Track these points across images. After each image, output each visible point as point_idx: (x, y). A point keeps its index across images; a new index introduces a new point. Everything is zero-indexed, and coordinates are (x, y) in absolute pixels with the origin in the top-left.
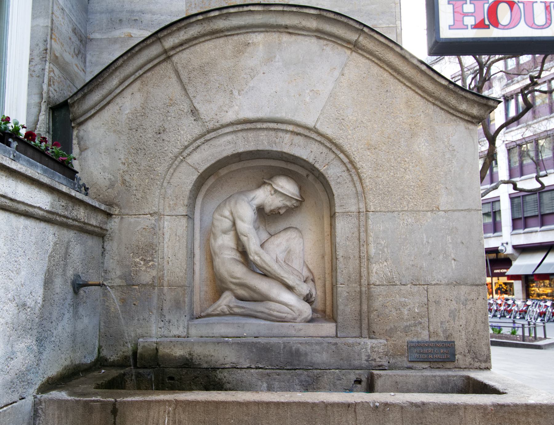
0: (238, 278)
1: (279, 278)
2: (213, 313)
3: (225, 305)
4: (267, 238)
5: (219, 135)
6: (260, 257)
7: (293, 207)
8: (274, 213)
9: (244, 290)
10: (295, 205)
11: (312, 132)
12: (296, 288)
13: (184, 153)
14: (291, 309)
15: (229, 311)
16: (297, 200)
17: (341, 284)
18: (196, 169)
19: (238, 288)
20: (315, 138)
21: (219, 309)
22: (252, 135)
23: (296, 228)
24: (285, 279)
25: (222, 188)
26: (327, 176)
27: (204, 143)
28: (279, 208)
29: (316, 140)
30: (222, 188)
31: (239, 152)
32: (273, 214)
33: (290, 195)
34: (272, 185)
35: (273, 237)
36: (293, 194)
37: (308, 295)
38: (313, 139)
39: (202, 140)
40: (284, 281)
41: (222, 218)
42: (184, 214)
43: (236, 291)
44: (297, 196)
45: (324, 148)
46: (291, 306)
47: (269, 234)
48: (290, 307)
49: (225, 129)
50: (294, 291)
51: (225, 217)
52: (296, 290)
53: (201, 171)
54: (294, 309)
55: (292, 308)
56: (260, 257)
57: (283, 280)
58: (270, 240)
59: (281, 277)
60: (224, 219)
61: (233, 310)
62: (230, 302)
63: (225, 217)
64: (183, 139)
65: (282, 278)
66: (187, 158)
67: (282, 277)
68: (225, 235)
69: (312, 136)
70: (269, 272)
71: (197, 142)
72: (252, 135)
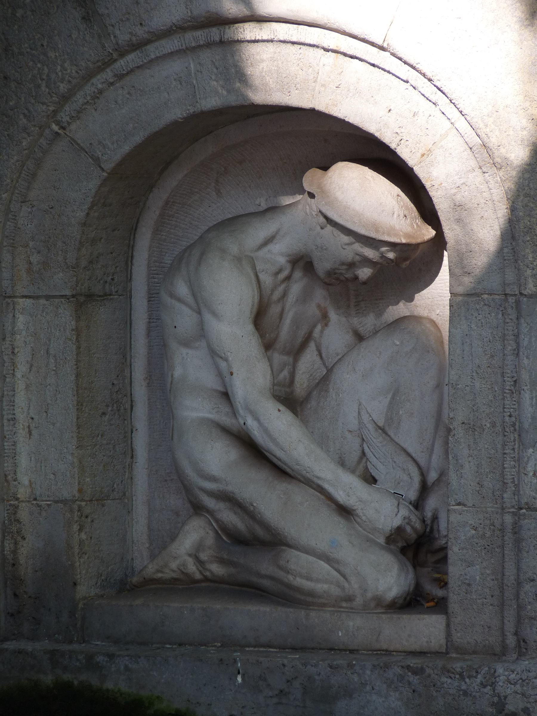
0: (213, 479)
1: (313, 482)
2: (160, 575)
12: (359, 512)
13: (62, 114)
17: (459, 504)
21: (174, 565)
25: (218, 192)
27: (112, 84)
30: (218, 192)
39: (108, 74)
41: (173, 301)
42: (68, 293)
46: (338, 562)
48: (336, 566)
50: (356, 518)
51: (179, 300)
55: (342, 568)
60: (178, 305)
61: (207, 570)
62: (200, 546)
63: (179, 300)
64: (53, 76)
66: (73, 127)
67: (318, 478)
68: (190, 352)
71: (94, 80)
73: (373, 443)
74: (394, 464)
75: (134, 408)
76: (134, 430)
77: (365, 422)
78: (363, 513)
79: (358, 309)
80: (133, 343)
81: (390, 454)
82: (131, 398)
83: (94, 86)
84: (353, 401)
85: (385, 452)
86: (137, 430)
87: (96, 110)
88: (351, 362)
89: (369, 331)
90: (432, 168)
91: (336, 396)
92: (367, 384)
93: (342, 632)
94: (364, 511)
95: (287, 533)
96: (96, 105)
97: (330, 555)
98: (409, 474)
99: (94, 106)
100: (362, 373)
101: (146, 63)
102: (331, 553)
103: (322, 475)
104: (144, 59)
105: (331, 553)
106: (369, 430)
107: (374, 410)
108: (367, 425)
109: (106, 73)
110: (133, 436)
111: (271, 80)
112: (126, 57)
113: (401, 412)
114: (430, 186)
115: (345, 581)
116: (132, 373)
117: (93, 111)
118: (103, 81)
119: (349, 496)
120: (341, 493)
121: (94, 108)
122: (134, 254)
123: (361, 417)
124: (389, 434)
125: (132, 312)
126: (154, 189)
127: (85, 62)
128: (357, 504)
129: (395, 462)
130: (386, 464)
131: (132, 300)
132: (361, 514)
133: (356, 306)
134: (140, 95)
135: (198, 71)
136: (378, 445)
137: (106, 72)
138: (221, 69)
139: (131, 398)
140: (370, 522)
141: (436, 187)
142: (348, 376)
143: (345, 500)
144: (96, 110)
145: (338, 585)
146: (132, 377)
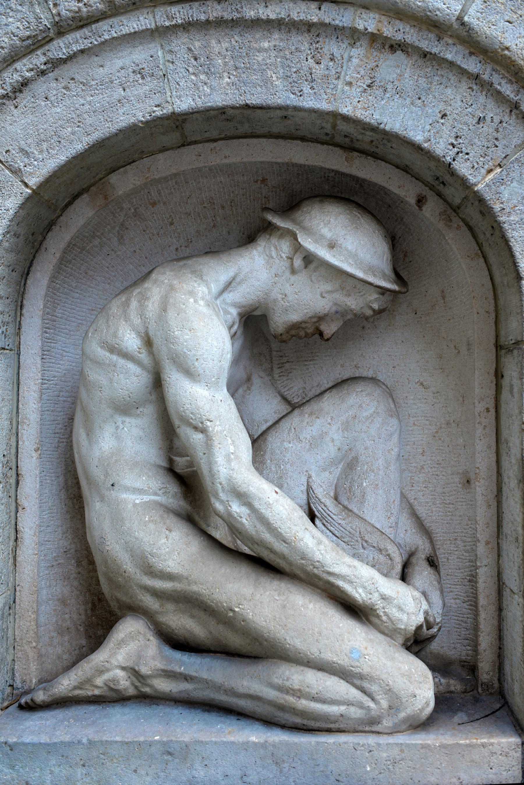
3: (123, 668)
4: (276, 417)
5: (103, 43)
6: (249, 505)
7: (369, 313)
8: (302, 333)
9: (192, 616)
10: (376, 306)
11: (450, 41)
14: (363, 691)
15: (136, 687)
16: (383, 291)
18: (16, 172)
19: (170, 606)
20: (459, 60)
22: (225, 45)
23: (374, 380)
24: (341, 583)
25: (121, 239)
26: (497, 207)
27: (43, 73)
28: (321, 318)
29: (463, 72)
30: (121, 239)
31: (177, 110)
32: (300, 338)
33: (360, 274)
34: (295, 237)
35: (296, 412)
36: (371, 269)
37: (419, 628)
38: (452, 64)
40: (338, 587)
43: (162, 619)
44: (384, 277)
45: (491, 104)
46: (361, 677)
47: (285, 399)
48: (358, 682)
49: (123, 19)
50: (373, 619)
52: (378, 616)
53: (33, 181)
54: (374, 688)
55: (366, 685)
56: (249, 505)
57: (332, 585)
58: (285, 424)
59: (325, 576)
65: (332, 579)
69: (449, 56)
70: (283, 557)
71: (18, 65)
72: (225, 45)
73: (332, 521)
74: (365, 544)
75: (20, 483)
76: (20, 509)
77: (320, 497)
78: (384, 612)
79: (282, 372)
80: (20, 406)
81: (358, 532)
82: (17, 471)
83: (18, 74)
84: (300, 473)
85: (351, 530)
86: (24, 508)
87: (16, 107)
88: (293, 429)
89: (297, 395)
90: (502, 188)
91: (276, 467)
92: (318, 454)
93: (370, 766)
94: (387, 610)
95: (289, 644)
96: (17, 100)
97: (351, 670)
98: (389, 555)
99: (14, 102)
100: (309, 441)
101: (95, 45)
102: (352, 667)
103: (336, 570)
104: (93, 40)
105: (352, 667)
106: (325, 506)
107: (324, 482)
108: (323, 500)
109: (37, 57)
110: (18, 515)
111: (274, 75)
112: (68, 36)
113: (365, 484)
114: (499, 209)
115: (369, 699)
116: (19, 442)
117: (12, 108)
118: (31, 66)
119: (371, 594)
120: (360, 590)
121: (14, 105)
122: (25, 302)
123: (313, 491)
124: (350, 508)
125: (21, 371)
126: (53, 227)
127: (10, 37)
128: (379, 602)
129: (366, 541)
130: (352, 544)
131: (21, 357)
132: (382, 614)
133: (279, 368)
134: (83, 90)
135: (168, 61)
136: (340, 522)
137: (37, 55)
138: (202, 59)
139: (17, 471)
140: (392, 622)
141: (508, 210)
142: (291, 446)
143: (365, 599)
144: (16, 107)
145: (361, 705)
146: (19, 446)
